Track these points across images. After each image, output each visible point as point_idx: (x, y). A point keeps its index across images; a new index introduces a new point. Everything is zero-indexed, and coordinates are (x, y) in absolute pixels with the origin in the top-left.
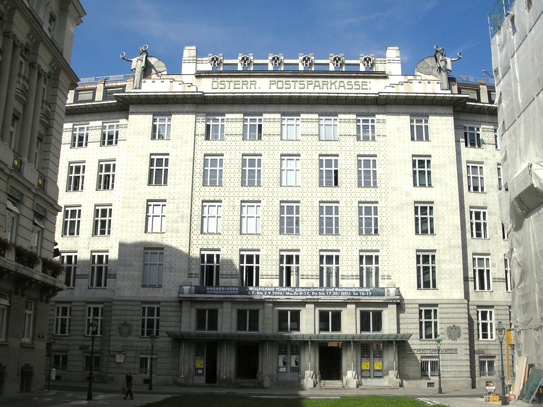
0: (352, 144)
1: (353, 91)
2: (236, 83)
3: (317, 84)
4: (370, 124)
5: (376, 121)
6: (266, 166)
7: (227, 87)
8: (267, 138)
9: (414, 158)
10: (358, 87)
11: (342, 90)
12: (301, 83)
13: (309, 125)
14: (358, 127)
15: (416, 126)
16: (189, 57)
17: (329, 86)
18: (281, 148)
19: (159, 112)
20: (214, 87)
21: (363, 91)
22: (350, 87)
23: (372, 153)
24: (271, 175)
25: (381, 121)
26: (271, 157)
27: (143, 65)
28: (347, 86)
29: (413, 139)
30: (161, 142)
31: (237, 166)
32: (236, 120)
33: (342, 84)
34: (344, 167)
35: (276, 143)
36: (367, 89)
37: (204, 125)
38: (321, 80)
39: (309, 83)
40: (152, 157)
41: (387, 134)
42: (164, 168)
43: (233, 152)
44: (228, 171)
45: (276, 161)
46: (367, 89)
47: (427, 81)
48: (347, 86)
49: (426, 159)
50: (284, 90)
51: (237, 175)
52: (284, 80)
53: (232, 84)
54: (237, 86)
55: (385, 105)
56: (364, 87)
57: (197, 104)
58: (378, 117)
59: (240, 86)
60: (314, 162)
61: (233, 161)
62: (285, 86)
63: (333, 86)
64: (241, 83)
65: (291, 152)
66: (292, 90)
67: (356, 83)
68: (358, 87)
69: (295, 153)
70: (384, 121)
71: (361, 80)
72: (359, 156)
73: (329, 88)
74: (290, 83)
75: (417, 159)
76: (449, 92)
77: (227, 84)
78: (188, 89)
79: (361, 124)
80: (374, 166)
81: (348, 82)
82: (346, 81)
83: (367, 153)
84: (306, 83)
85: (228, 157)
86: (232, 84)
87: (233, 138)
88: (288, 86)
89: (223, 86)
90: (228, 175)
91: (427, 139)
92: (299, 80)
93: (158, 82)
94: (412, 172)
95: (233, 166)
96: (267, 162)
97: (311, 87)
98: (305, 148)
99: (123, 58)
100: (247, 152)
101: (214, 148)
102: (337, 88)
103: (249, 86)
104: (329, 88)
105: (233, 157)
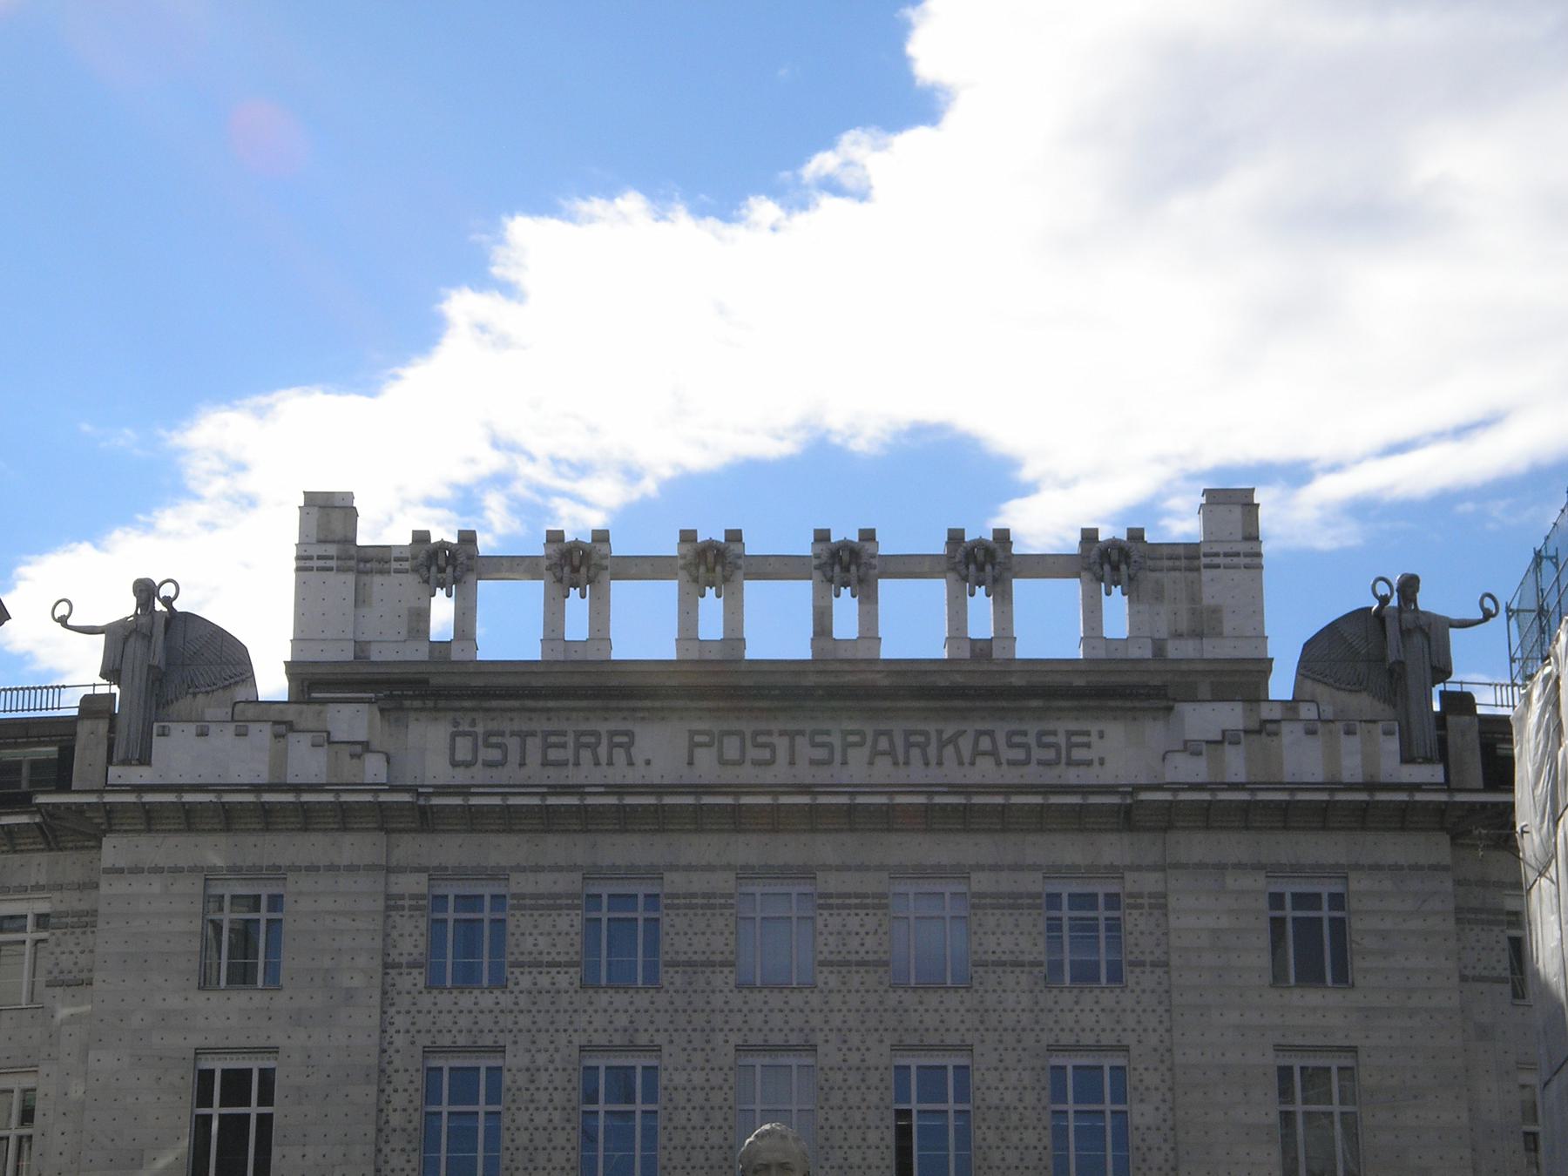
0: (1026, 1000)
1: (1032, 774)
2: (553, 739)
3: (883, 744)
4: (1102, 914)
5: (1126, 901)
6: (680, 1098)
7: (514, 757)
8: (678, 979)
9: (1285, 1061)
10: (1050, 754)
11: (985, 771)
12: (819, 739)
13: (853, 923)
14: (1054, 926)
15: (1295, 919)
16: (320, 541)
17: (932, 751)
18: (737, 1020)
19: (234, 869)
20: (459, 757)
21: (1072, 776)
22: (1020, 754)
23: (1108, 1039)
24: (698, 1138)
25: (1146, 901)
26: (698, 1058)
27: (158, 658)
28: (1007, 754)
29: (1278, 978)
30: (240, 999)
31: (559, 1097)
32: (550, 903)
33: (985, 744)
34: (993, 1098)
35: (717, 1001)
36: (1089, 763)
37: (423, 924)
38: (898, 727)
39: (851, 739)
40: (206, 1064)
41: (1175, 960)
42: (254, 1110)
43: (543, 1040)
44: (522, 1118)
45: (716, 1079)
46: (1089, 763)
47: (1340, 726)
48: (1007, 754)
49: (1333, 1062)
50: (747, 774)
51: (560, 1138)
52: (747, 727)
53: (534, 745)
54: (553, 754)
55: (1165, 830)
56: (1078, 754)
57: (388, 831)
58: (1132, 883)
59: (568, 754)
60: (873, 1078)
61: (543, 1078)
62: (753, 753)
63: (949, 751)
64: (570, 740)
65: (776, 1039)
66: (780, 773)
67: (1047, 739)
68: (1050, 754)
69: (794, 1039)
70: (1160, 903)
71: (1063, 726)
72: (1054, 1049)
73: (933, 761)
74: (776, 740)
75: (1296, 1062)
76: (1434, 773)
77: (513, 743)
78: (349, 770)
79: (1066, 913)
80: (1120, 1095)
81: (1015, 733)
82: (1001, 729)
83: (1088, 1039)
84: (836, 740)
85: (524, 1060)
86: (534, 745)
87: (544, 981)
88: (766, 754)
89: (495, 754)
90: (522, 1138)
91: (1342, 976)
92: (808, 726)
93: (223, 737)
94: (1274, 1118)
95: (543, 1097)
96: (680, 1079)
97: (858, 756)
98: (836, 1020)
99: (63, 621)
100: (600, 1039)
101: (464, 1021)
102: (967, 759)
103: (603, 751)
104: (933, 761)
105: (541, 1059)
